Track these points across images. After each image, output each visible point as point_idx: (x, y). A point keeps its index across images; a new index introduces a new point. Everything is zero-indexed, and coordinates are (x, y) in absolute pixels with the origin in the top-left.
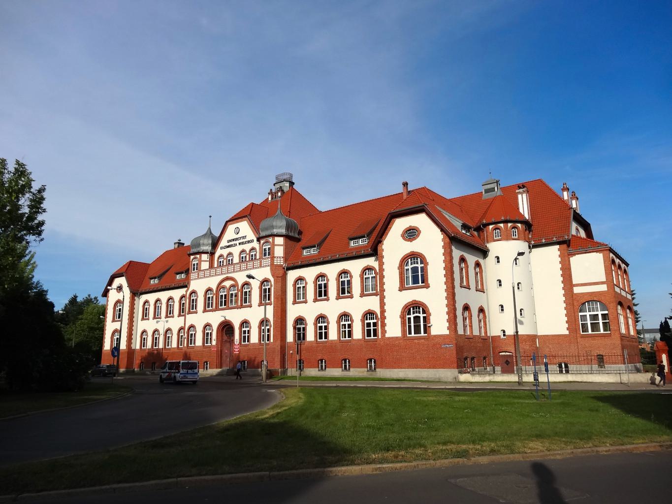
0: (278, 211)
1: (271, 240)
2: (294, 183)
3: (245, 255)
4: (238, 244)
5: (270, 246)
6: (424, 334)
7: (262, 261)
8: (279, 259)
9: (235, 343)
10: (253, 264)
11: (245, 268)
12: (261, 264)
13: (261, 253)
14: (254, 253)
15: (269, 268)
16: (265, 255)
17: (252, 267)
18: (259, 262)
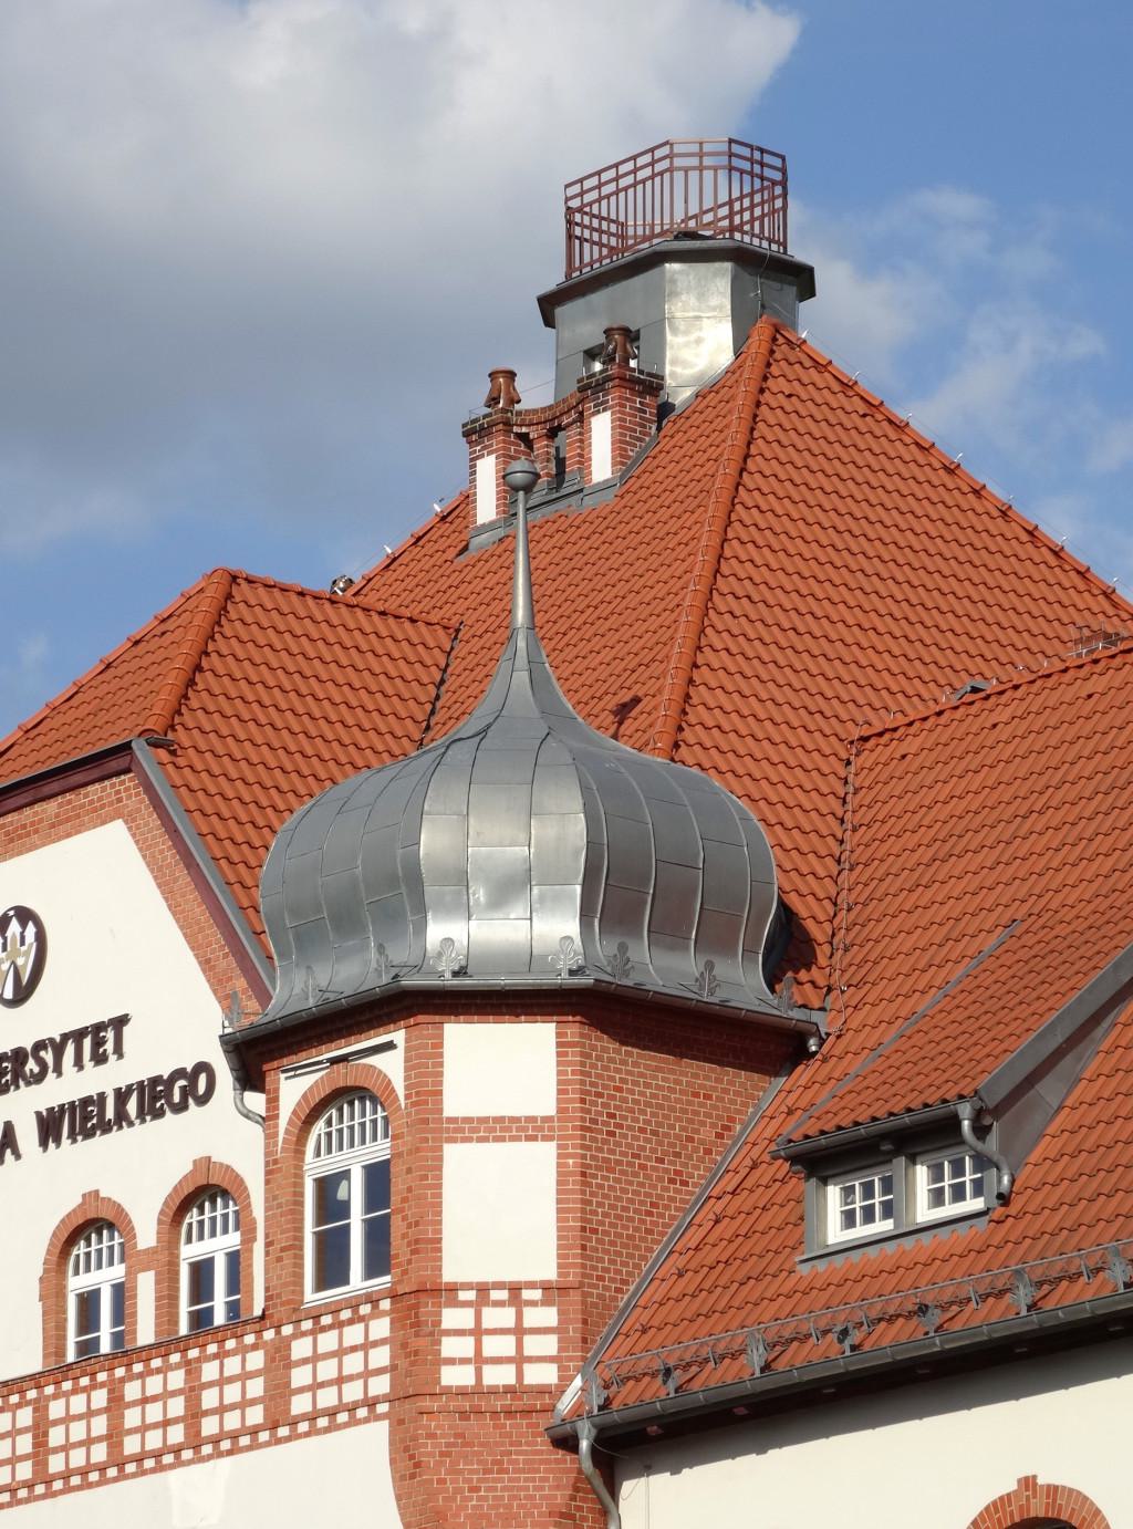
0: (513, 680)
1: (392, 1066)
2: (802, 280)
3: (118, 1272)
4: (27, 1135)
5: (380, 1150)
7: (300, 1349)
8: (506, 1317)
10: (192, 1392)
11: (100, 1453)
12: (279, 1392)
13: (284, 1250)
14: (217, 1247)
15: (376, 1437)
16: (332, 1269)
17: (177, 1434)
18: (256, 1360)
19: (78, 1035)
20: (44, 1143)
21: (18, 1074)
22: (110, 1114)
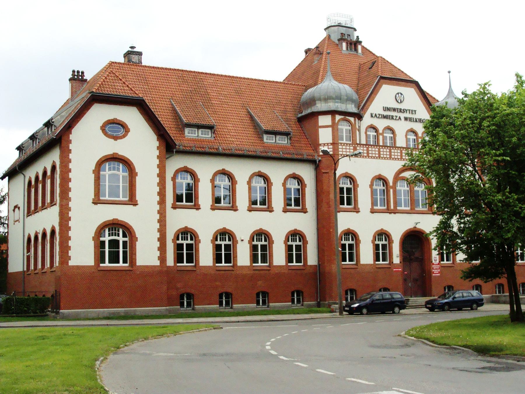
4: (403, 119)
6: (123, 263)
9: (433, 262)
19: (409, 110)
20: (405, 120)
21: (401, 111)
22: (415, 120)
